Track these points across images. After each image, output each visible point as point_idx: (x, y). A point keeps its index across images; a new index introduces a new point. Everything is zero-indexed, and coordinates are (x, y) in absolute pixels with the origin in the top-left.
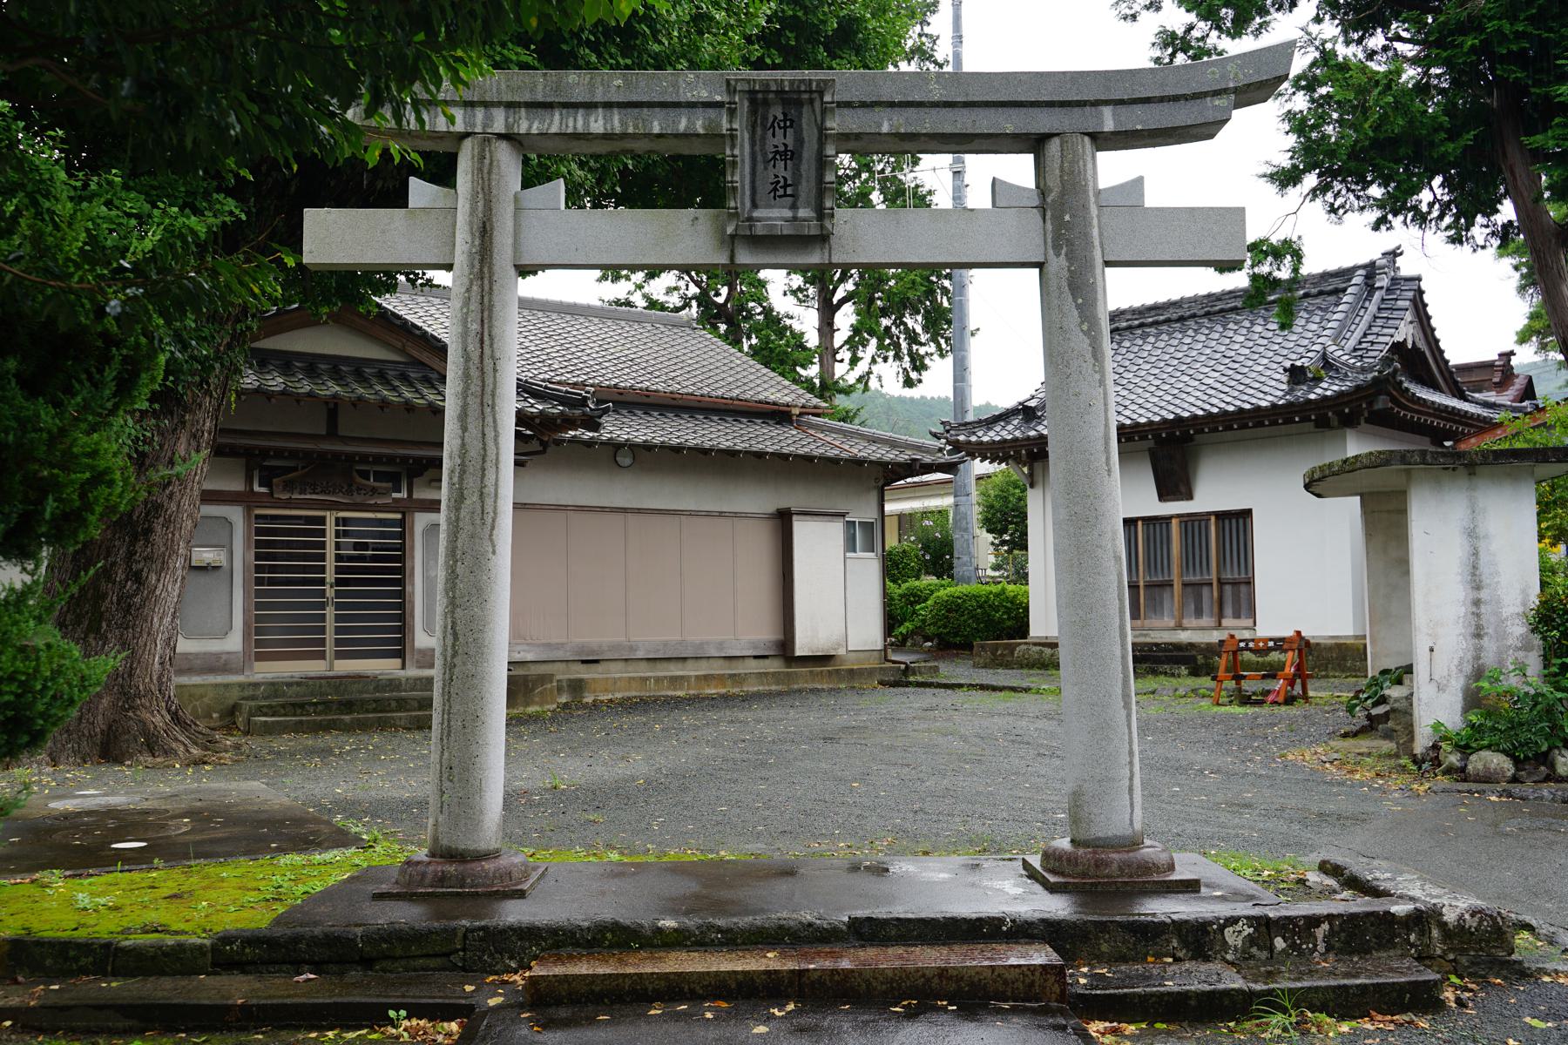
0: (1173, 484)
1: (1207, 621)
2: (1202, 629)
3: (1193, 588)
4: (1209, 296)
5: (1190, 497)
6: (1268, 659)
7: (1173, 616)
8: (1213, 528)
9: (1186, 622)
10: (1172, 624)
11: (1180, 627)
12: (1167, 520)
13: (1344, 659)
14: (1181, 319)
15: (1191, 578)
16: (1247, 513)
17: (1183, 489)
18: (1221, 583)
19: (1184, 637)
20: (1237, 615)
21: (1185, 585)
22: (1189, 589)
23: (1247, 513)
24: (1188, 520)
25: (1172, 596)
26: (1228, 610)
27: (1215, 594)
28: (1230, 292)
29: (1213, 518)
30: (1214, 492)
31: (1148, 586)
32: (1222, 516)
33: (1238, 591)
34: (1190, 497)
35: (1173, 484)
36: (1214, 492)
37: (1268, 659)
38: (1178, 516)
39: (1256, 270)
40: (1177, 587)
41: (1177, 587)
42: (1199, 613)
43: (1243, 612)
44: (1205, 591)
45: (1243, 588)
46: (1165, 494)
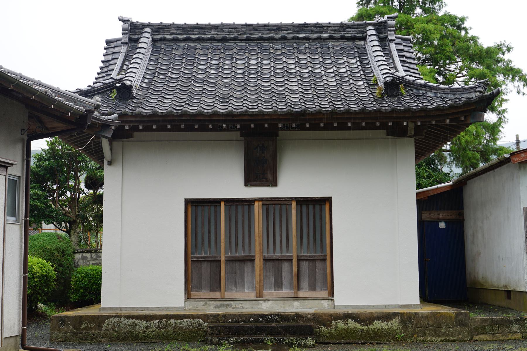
0: (260, 171)
1: (285, 292)
2: (284, 299)
3: (274, 263)
4: (246, 25)
5: (274, 183)
6: (372, 327)
7: (253, 288)
8: (294, 212)
9: (266, 293)
10: (253, 295)
11: (260, 297)
12: (249, 202)
13: (439, 326)
14: (224, 40)
15: (271, 254)
16: (328, 200)
17: (270, 176)
18: (299, 260)
19: (266, 307)
20: (313, 287)
21: (266, 260)
22: (270, 264)
23: (328, 200)
24: (269, 204)
25: (253, 270)
26: (305, 283)
27: (295, 269)
28: (265, 26)
29: (294, 204)
30: (296, 181)
31: (229, 261)
32: (302, 202)
33: (317, 265)
34: (274, 183)
35: (260, 171)
36: (296, 181)
37: (372, 327)
38: (262, 200)
39: (131, 36)
40: (258, 262)
41: (258, 262)
42: (278, 285)
43: (318, 284)
44: (285, 266)
45: (319, 264)
46: (251, 180)
